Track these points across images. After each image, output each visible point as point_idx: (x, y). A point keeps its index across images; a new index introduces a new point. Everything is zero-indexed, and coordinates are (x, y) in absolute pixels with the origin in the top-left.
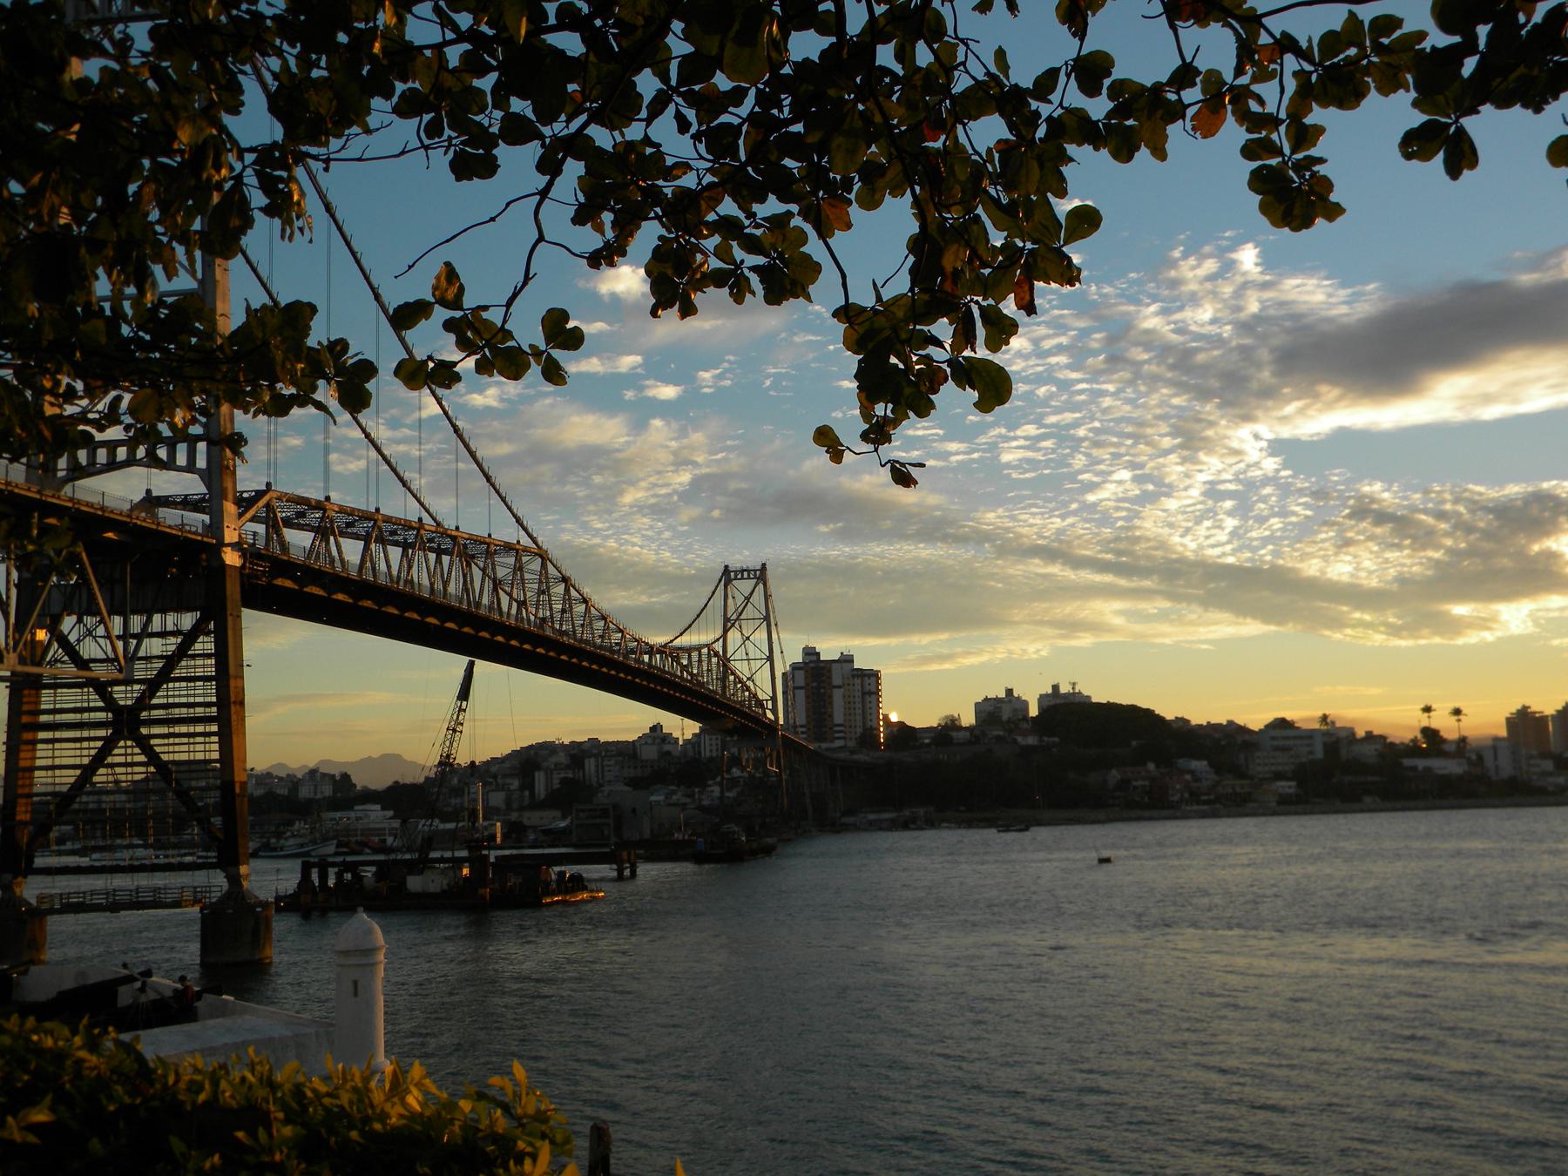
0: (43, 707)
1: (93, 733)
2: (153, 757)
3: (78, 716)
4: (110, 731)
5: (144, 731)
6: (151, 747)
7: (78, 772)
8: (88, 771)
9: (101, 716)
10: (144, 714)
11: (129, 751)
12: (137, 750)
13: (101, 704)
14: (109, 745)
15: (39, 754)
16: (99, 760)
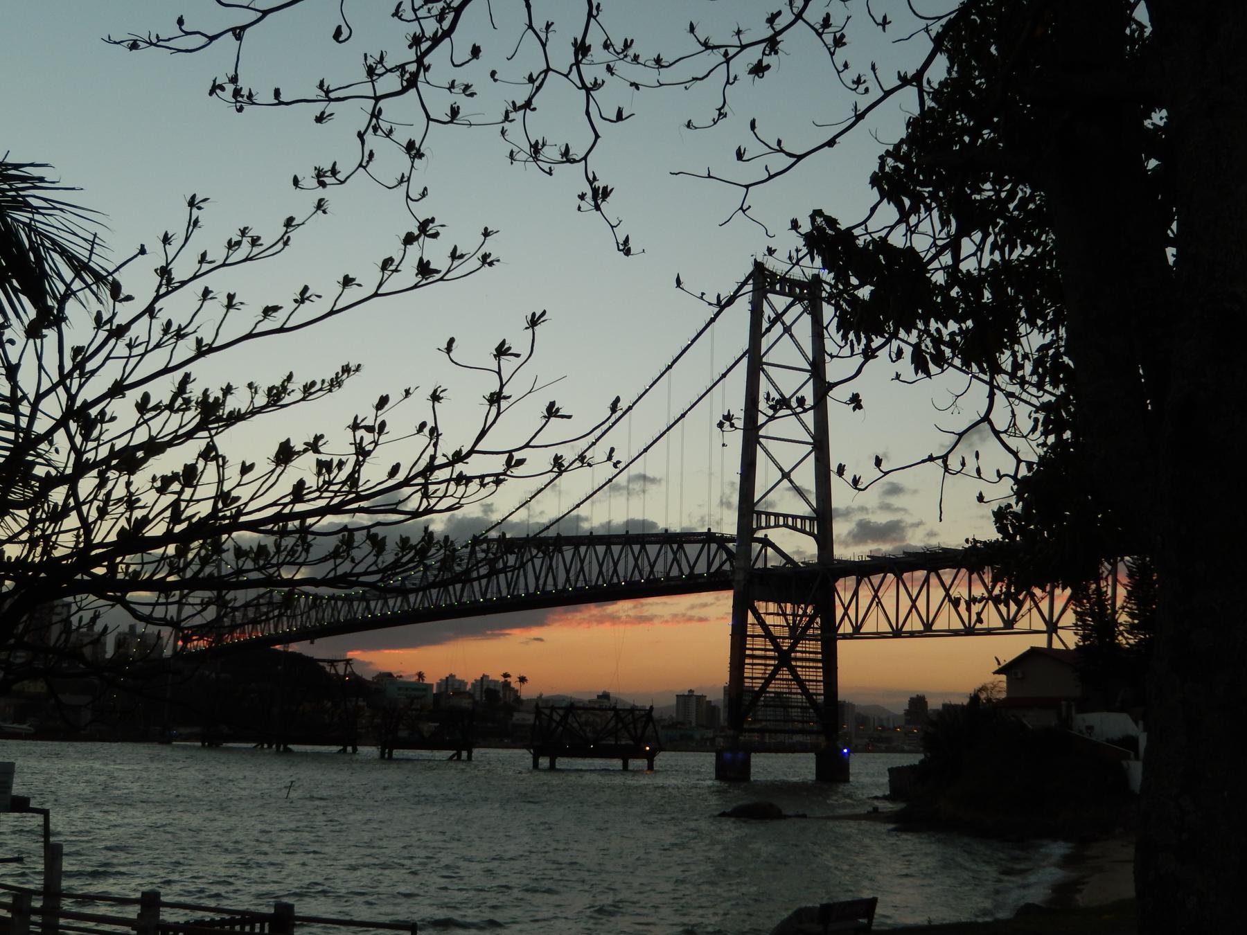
0: (748, 646)
1: (768, 662)
2: (796, 677)
3: (763, 653)
4: (776, 662)
5: (794, 663)
6: (796, 671)
7: (763, 681)
8: (768, 681)
9: (772, 653)
10: (793, 655)
11: (804, 673)
12: (799, 673)
13: (772, 648)
14: (777, 669)
15: (746, 670)
16: (772, 676)
